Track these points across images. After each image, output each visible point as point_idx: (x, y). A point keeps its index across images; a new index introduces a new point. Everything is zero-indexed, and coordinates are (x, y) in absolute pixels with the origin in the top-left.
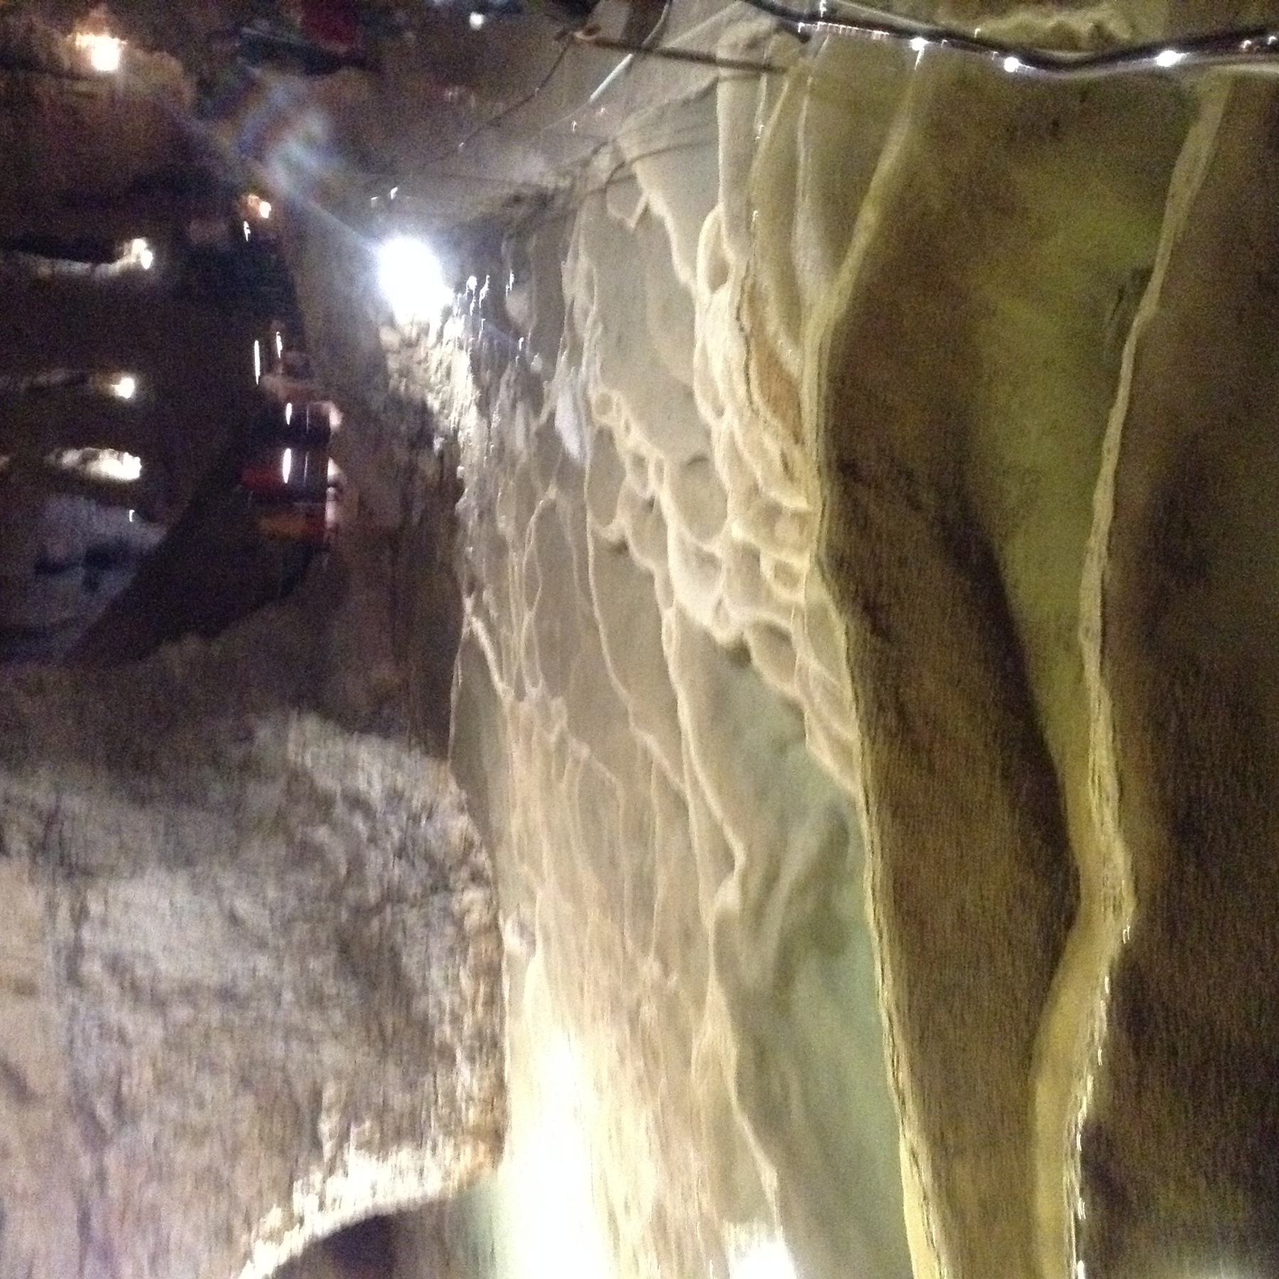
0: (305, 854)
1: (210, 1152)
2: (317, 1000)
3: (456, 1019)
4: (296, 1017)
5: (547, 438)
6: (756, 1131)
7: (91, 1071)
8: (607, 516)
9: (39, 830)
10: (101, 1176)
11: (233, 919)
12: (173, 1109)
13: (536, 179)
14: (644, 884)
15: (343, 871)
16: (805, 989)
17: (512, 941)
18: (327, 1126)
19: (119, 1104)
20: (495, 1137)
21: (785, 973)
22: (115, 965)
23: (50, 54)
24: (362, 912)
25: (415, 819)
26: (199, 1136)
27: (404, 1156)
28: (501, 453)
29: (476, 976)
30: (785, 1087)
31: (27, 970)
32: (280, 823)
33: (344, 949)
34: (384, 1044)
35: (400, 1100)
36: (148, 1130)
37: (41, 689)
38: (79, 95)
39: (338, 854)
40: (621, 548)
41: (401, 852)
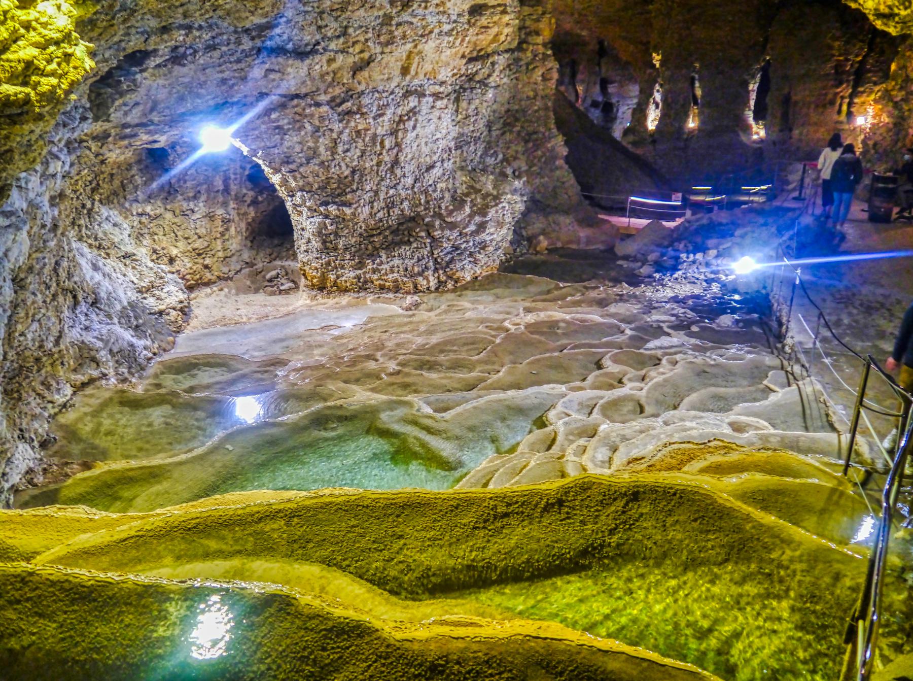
0: (458, 202)
1: (324, 154)
2: (390, 206)
3: (374, 271)
4: (382, 196)
5: (657, 331)
6: (313, 413)
7: (366, 100)
8: (616, 360)
9: (477, 78)
10: (318, 105)
12: (345, 137)
13: (789, 334)
14: (432, 366)
15: (449, 220)
16: (377, 444)
17: (409, 299)
18: (332, 208)
19: (349, 113)
20: (321, 287)
21: (385, 433)
22: (413, 112)
24: (429, 228)
25: (471, 255)
26: (333, 150)
27: (316, 244)
28: (650, 307)
29: (396, 281)
30: (333, 429)
31: (413, 72)
32: (473, 189)
33: (412, 219)
34: (368, 235)
35: (341, 243)
36: (337, 127)
37: (545, 78)
38: (841, 105)
39: (459, 217)
40: (599, 366)
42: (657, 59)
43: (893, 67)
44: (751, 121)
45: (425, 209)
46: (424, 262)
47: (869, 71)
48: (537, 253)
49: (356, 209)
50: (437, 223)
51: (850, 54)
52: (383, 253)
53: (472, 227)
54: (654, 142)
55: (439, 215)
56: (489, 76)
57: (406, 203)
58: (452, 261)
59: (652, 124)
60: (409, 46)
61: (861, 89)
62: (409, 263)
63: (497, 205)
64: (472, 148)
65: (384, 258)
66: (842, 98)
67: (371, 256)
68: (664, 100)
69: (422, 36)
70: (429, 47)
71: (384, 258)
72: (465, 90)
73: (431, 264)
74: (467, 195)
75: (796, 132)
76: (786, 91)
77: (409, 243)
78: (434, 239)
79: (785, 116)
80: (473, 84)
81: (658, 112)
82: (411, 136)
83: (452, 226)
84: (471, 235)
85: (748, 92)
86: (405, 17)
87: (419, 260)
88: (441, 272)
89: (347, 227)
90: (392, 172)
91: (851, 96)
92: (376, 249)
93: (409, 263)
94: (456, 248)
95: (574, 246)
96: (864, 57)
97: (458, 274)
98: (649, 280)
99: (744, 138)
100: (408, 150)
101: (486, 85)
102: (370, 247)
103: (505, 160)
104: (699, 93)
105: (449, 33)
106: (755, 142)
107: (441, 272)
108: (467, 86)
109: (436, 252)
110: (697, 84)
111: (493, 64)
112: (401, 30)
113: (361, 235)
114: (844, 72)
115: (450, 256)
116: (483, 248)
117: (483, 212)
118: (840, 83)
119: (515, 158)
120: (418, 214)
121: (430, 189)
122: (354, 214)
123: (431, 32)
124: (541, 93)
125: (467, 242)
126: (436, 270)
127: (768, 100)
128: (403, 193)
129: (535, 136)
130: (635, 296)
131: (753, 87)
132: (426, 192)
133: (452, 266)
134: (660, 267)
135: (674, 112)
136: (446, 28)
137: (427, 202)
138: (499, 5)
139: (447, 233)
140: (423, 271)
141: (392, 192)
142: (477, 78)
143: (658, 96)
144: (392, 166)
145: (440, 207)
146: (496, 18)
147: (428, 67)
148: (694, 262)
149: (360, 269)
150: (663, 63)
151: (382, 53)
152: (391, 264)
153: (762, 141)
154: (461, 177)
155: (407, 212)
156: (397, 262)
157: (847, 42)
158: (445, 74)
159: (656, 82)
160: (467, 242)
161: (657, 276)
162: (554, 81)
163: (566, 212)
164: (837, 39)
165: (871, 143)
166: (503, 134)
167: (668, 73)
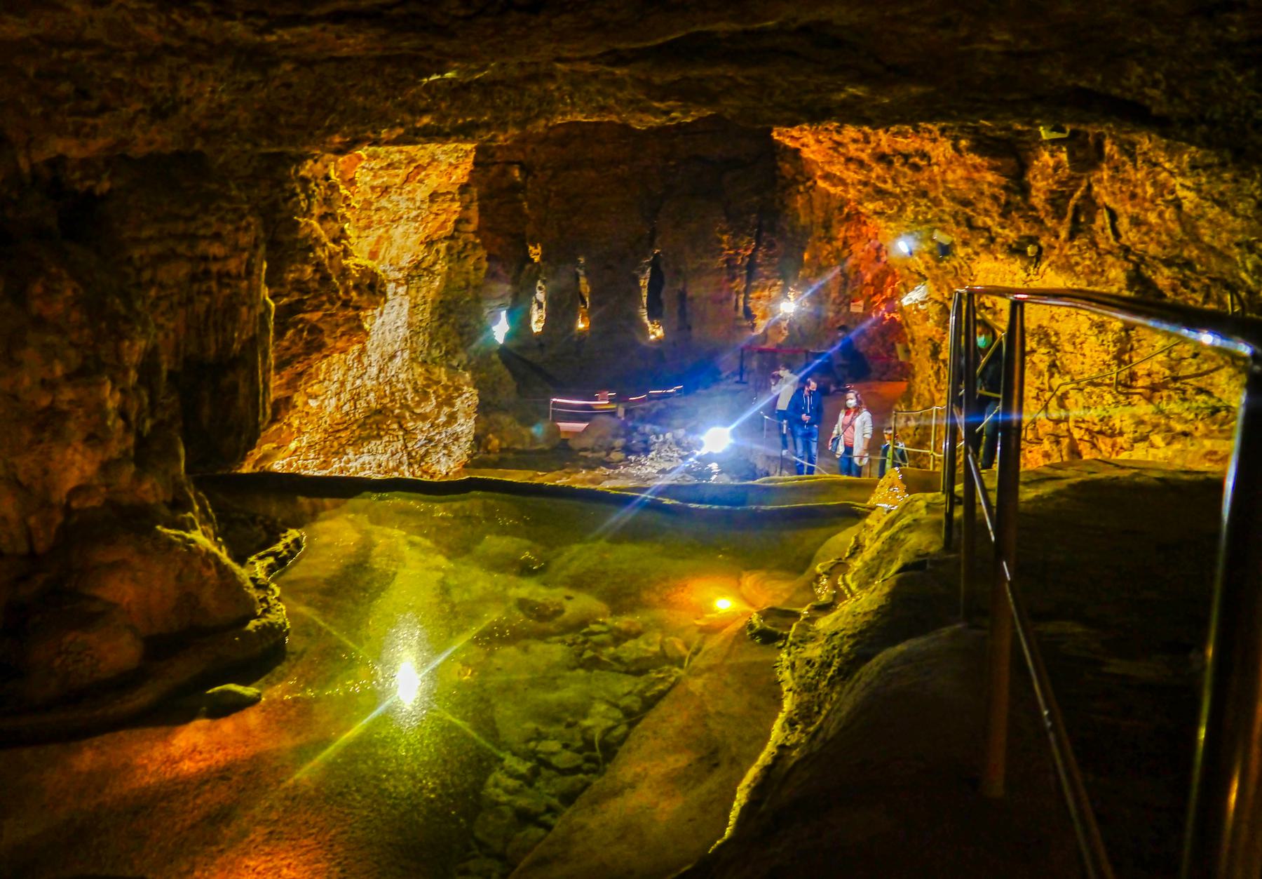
2: (355, 398)
4: (349, 387)
9: (424, 265)
11: (392, 357)
15: (418, 411)
23: (757, 287)
24: (400, 420)
25: (445, 447)
31: (381, 257)
32: (431, 381)
33: (379, 412)
34: (333, 432)
37: (476, 269)
38: (737, 301)
39: (429, 407)
41: (430, 440)
42: (535, 253)
43: (806, 256)
44: (645, 319)
45: (391, 401)
46: (398, 456)
47: (760, 265)
48: (489, 452)
49: (323, 401)
50: (407, 414)
51: (739, 248)
52: (350, 450)
53: (443, 419)
54: (541, 346)
55: (408, 407)
56: (434, 263)
57: (372, 395)
58: (427, 453)
59: (537, 327)
60: (383, 230)
61: (754, 284)
62: (383, 458)
63: (460, 395)
64: (421, 338)
65: (351, 456)
66: (738, 293)
67: (336, 453)
68: (550, 299)
69: (393, 221)
70: (397, 232)
71: (351, 456)
72: (413, 278)
73: (405, 458)
74: (429, 386)
75: (695, 332)
76: (680, 286)
77: (379, 437)
78: (406, 431)
79: (682, 314)
80: (420, 272)
81: (543, 313)
82: (378, 322)
83: (424, 417)
84: (443, 425)
85: (639, 289)
86: (384, 202)
87: (393, 455)
88: (416, 466)
89: (311, 422)
90: (359, 361)
91: (747, 291)
92: (341, 445)
93: (383, 458)
94: (430, 440)
95: (519, 447)
96: (754, 250)
97: (434, 468)
98: (628, 463)
99: (640, 339)
100: (375, 338)
101: (433, 273)
102: (335, 444)
103: (447, 353)
104: (585, 287)
105: (415, 219)
106: (651, 342)
107: (416, 466)
108: (414, 273)
109: (409, 445)
110: (583, 281)
111: (438, 251)
112: (380, 213)
113: (325, 431)
114: (736, 266)
115: (424, 449)
116: (457, 439)
117: (449, 401)
118: (733, 278)
119: (456, 352)
120: (384, 407)
121: (394, 379)
122: (320, 407)
123: (401, 218)
124: (473, 283)
125: (440, 433)
126: (410, 465)
127: (663, 296)
128: (369, 384)
129: (467, 329)
130: (620, 474)
131: (644, 282)
132: (390, 383)
133: (427, 459)
134: (628, 450)
135: (560, 310)
136: (414, 213)
137: (393, 394)
138: (448, 193)
139: (420, 424)
140: (398, 467)
141: (358, 382)
142: (424, 265)
143: (540, 296)
144: (360, 355)
145: (405, 399)
146: (445, 206)
147: (394, 252)
148: (664, 442)
149: (324, 469)
150: (543, 258)
151: (359, 237)
152: (361, 461)
153: (659, 341)
154: (419, 370)
155: (373, 405)
156: (366, 458)
157: (735, 236)
158: (405, 261)
159: (537, 278)
160: (440, 433)
161: (632, 458)
162: (483, 271)
163: (505, 411)
164: (725, 232)
165: (796, 327)
166: (441, 326)
167: (550, 269)
